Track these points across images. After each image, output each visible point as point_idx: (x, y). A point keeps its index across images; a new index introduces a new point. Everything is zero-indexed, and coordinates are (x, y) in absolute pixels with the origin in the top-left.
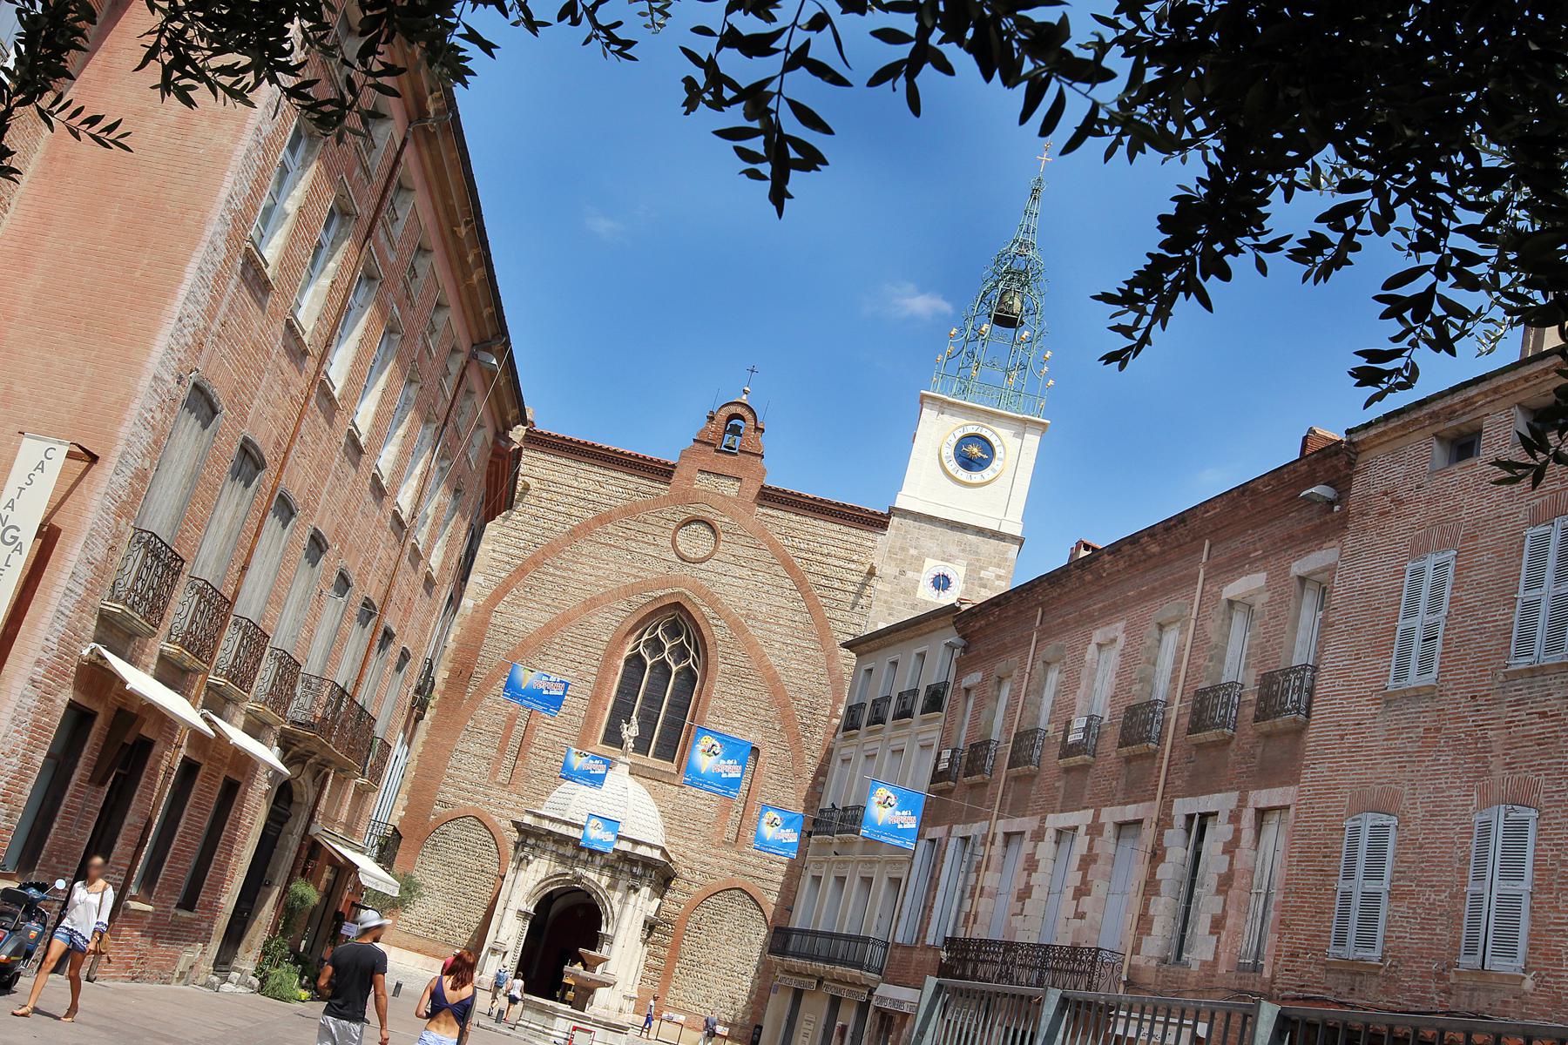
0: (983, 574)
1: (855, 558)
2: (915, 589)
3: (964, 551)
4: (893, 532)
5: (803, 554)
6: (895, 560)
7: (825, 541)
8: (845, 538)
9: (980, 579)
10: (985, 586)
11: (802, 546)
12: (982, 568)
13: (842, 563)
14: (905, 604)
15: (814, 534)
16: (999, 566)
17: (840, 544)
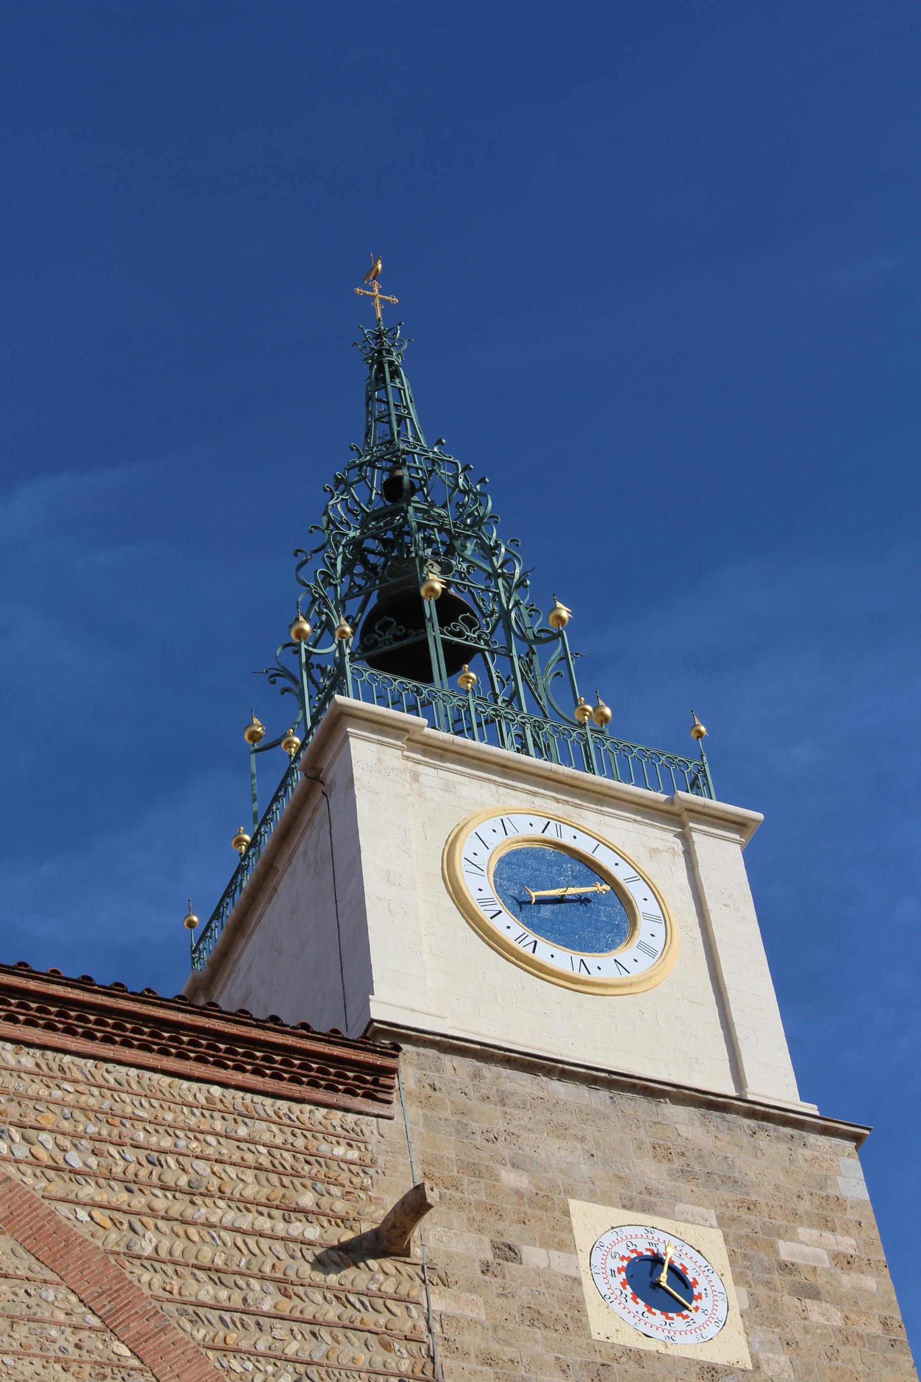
0: (786, 1250)
1: (307, 1200)
2: (578, 1306)
3: (686, 1174)
4: (414, 1112)
5: (88, 1191)
6: (461, 1206)
7: (167, 1143)
8: (242, 1132)
9: (787, 1268)
10: (810, 1292)
11: (75, 1160)
12: (778, 1232)
13: (264, 1223)
15: (110, 1116)
16: (827, 1224)
17: (227, 1149)
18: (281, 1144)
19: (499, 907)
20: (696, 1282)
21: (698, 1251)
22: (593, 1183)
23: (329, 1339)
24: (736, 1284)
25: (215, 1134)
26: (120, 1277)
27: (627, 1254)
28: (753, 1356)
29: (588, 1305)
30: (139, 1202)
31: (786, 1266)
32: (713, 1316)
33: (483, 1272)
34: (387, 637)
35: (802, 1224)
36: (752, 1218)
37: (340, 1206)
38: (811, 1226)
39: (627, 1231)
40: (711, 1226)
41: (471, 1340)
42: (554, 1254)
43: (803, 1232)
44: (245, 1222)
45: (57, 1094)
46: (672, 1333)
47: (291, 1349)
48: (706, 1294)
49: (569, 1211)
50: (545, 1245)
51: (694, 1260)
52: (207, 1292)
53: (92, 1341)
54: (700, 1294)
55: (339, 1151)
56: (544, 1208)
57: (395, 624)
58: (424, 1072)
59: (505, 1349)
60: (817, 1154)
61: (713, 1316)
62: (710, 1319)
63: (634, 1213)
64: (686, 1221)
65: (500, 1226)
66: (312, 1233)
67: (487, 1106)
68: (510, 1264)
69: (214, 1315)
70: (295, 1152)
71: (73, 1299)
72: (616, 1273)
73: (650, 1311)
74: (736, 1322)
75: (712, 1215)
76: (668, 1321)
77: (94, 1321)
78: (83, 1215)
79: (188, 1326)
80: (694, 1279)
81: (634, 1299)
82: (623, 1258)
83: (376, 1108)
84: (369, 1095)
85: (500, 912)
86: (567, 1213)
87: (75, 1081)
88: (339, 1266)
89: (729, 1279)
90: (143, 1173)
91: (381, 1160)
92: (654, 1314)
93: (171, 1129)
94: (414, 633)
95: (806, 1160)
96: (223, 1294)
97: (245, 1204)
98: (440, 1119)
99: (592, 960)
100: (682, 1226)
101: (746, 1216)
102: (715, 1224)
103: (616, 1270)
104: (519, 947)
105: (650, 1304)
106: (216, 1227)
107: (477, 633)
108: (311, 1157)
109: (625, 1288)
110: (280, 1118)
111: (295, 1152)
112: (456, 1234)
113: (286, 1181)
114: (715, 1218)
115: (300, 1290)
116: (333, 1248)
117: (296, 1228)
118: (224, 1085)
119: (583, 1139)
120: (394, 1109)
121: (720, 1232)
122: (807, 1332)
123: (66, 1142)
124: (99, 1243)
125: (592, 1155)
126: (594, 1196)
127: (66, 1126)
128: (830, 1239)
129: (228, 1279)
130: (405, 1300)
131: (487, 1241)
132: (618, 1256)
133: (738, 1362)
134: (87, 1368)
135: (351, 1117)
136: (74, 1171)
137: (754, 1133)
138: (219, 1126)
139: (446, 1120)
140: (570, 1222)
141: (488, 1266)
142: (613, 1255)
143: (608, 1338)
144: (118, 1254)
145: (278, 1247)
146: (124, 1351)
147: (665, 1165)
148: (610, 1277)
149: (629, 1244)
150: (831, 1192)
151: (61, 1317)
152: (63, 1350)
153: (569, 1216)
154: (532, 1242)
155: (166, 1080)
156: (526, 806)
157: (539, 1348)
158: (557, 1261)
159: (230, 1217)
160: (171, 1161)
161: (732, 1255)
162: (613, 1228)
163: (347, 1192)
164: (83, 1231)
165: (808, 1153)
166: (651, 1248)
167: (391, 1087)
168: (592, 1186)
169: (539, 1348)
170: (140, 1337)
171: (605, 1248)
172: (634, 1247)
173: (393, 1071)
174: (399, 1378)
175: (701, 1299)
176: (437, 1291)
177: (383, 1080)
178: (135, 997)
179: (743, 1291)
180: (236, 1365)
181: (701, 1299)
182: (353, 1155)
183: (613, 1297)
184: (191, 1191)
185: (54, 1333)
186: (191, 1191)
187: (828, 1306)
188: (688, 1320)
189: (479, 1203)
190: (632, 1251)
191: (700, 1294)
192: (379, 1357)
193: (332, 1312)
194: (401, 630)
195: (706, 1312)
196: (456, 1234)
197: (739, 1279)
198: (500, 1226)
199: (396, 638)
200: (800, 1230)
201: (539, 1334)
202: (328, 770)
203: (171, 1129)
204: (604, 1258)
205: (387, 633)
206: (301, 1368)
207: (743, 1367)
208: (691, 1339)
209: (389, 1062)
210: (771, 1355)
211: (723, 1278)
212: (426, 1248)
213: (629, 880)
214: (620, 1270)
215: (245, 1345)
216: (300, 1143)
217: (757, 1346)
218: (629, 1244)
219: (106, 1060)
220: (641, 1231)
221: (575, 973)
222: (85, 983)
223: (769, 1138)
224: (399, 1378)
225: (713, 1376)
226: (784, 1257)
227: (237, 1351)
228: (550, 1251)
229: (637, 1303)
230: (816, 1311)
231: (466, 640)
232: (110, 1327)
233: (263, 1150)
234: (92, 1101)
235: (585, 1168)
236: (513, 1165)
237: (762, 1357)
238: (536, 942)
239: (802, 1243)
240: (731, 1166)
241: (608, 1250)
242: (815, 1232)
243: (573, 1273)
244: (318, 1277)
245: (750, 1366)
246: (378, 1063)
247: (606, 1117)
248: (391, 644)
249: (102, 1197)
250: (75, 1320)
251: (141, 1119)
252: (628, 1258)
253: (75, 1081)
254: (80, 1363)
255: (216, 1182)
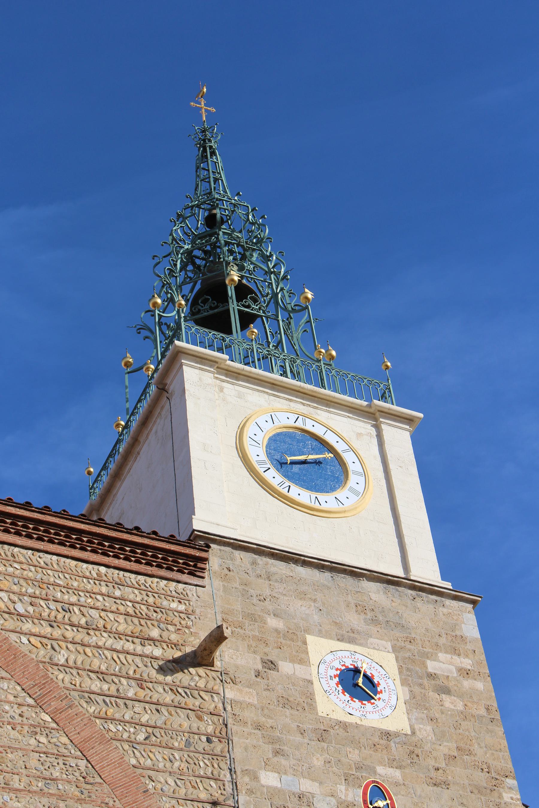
0: (432, 666)
1: (155, 633)
2: (311, 696)
3: (374, 621)
4: (217, 583)
5: (27, 626)
7: (74, 599)
8: (118, 593)
9: (432, 676)
11: (20, 608)
12: (427, 656)
13: (129, 646)
14: (302, 733)
16: (455, 651)
17: (109, 603)
18: (140, 601)
19: (268, 466)
20: (379, 684)
21: (381, 666)
22: (321, 626)
23: (166, 714)
24: (402, 685)
25: (102, 594)
26: (46, 676)
27: (340, 667)
28: (411, 726)
29: (316, 696)
30: (57, 633)
31: (431, 675)
32: (388, 703)
33: (256, 676)
34: (206, 307)
35: (441, 651)
36: (412, 647)
37: (174, 637)
38: (446, 652)
39: (340, 654)
40: (388, 652)
41: (248, 715)
42: (297, 666)
43: (441, 656)
44: (118, 645)
45: (10, 570)
46: (365, 713)
47: (145, 719)
48: (385, 690)
49: (306, 642)
50: (292, 661)
51: (378, 671)
52: (96, 685)
53: (29, 712)
54: (381, 691)
55: (174, 605)
56: (292, 640)
57: (211, 300)
58: (224, 560)
59: (268, 720)
60: (450, 611)
61: (388, 703)
62: (387, 705)
63: (343, 643)
64: (374, 648)
65: (266, 650)
66: (158, 652)
67: (260, 581)
68: (272, 672)
69: (100, 699)
70: (148, 606)
71: (19, 688)
72: (333, 678)
73: (352, 700)
74: (402, 706)
75: (389, 645)
76: (363, 706)
77: (30, 701)
78: (24, 640)
79: (85, 705)
80: (378, 682)
81: (343, 693)
82: (337, 669)
83: (195, 581)
84: (191, 573)
85: (269, 468)
86: (305, 643)
87: (21, 563)
88: (173, 672)
89: (398, 682)
90: (60, 616)
91: (198, 611)
92: (355, 702)
93: (76, 591)
94: (221, 305)
95: (444, 615)
96: (105, 687)
97: (119, 635)
98: (232, 588)
99: (322, 497)
100: (371, 651)
101: (409, 646)
102: (391, 650)
103: (333, 676)
104: (280, 489)
105: (352, 696)
106: (101, 648)
107: (258, 306)
108: (157, 608)
109: (338, 687)
110: (139, 585)
111: (148, 606)
112: (240, 654)
113: (143, 622)
114: (391, 647)
115: (150, 685)
116: (169, 661)
117: (148, 649)
118: (107, 566)
119: (315, 601)
120: (206, 582)
121: (394, 655)
122: (442, 713)
123: (15, 598)
124: (34, 656)
125: (320, 610)
126: (321, 634)
127: (15, 588)
128: (457, 660)
129: (109, 678)
130: (211, 692)
131: (258, 658)
132: (334, 668)
133: (402, 730)
134: (26, 728)
135: (181, 586)
136: (19, 615)
137: (414, 599)
138: (104, 590)
139: (236, 588)
140: (307, 648)
141: (259, 673)
142: (331, 667)
143: (328, 715)
144: (45, 662)
145: (138, 660)
146: (48, 718)
147: (362, 616)
148: (329, 680)
149: (341, 661)
150: (458, 633)
151: (11, 698)
152: (12, 717)
153: (306, 645)
154: (285, 659)
155: (74, 563)
156: (285, 407)
157: (288, 720)
158: (299, 671)
159: (110, 642)
160: (76, 609)
161: (400, 668)
162: (331, 652)
163: (178, 629)
164: (24, 649)
165: (445, 610)
166: (354, 663)
167: (204, 569)
168: (320, 627)
169: (288, 720)
170: (56, 710)
171: (327, 663)
172: (344, 663)
173: (204, 560)
174: (207, 736)
175: (382, 693)
176: (229, 687)
177: (199, 565)
178: (56, 514)
179: (406, 689)
180: (112, 727)
181: (382, 693)
182: (182, 607)
183: (331, 692)
184: (87, 627)
185: (7, 707)
186: (87, 627)
187: (455, 698)
188: (374, 705)
189: (254, 637)
190: (343, 665)
191: (381, 691)
192: (195, 724)
193: (168, 698)
194: (214, 304)
195: (385, 701)
196: (240, 654)
197: (404, 682)
198: (266, 650)
199: (211, 308)
200: (440, 655)
201: (288, 712)
202: (170, 384)
203: (76, 591)
204: (326, 669)
205: (206, 305)
206: (150, 730)
207: (405, 733)
208: (376, 716)
209: (203, 555)
210: (421, 726)
211: (395, 682)
212: (223, 662)
213: (344, 451)
214: (335, 676)
215: (117, 716)
216: (151, 600)
217: (414, 721)
218: (341, 661)
219: (39, 551)
220: (347, 654)
221: (312, 505)
222: (27, 506)
223: (423, 601)
224: (207, 736)
225: (388, 737)
226: (430, 670)
227: (113, 719)
228: (295, 665)
229: (345, 695)
230: (448, 701)
231: (252, 310)
232: (39, 705)
233: (130, 604)
234: (30, 574)
235: (316, 617)
236: (274, 615)
237: (416, 727)
238: (290, 486)
239: (441, 662)
240: (401, 618)
241: (328, 665)
242: (449, 656)
243: (308, 678)
244: (161, 678)
245: (409, 732)
246: (197, 555)
247: (329, 588)
248: (208, 311)
249: (36, 630)
250: (19, 700)
251: (59, 585)
252: (340, 670)
253: (21, 563)
254: (22, 725)
255: (102, 622)
